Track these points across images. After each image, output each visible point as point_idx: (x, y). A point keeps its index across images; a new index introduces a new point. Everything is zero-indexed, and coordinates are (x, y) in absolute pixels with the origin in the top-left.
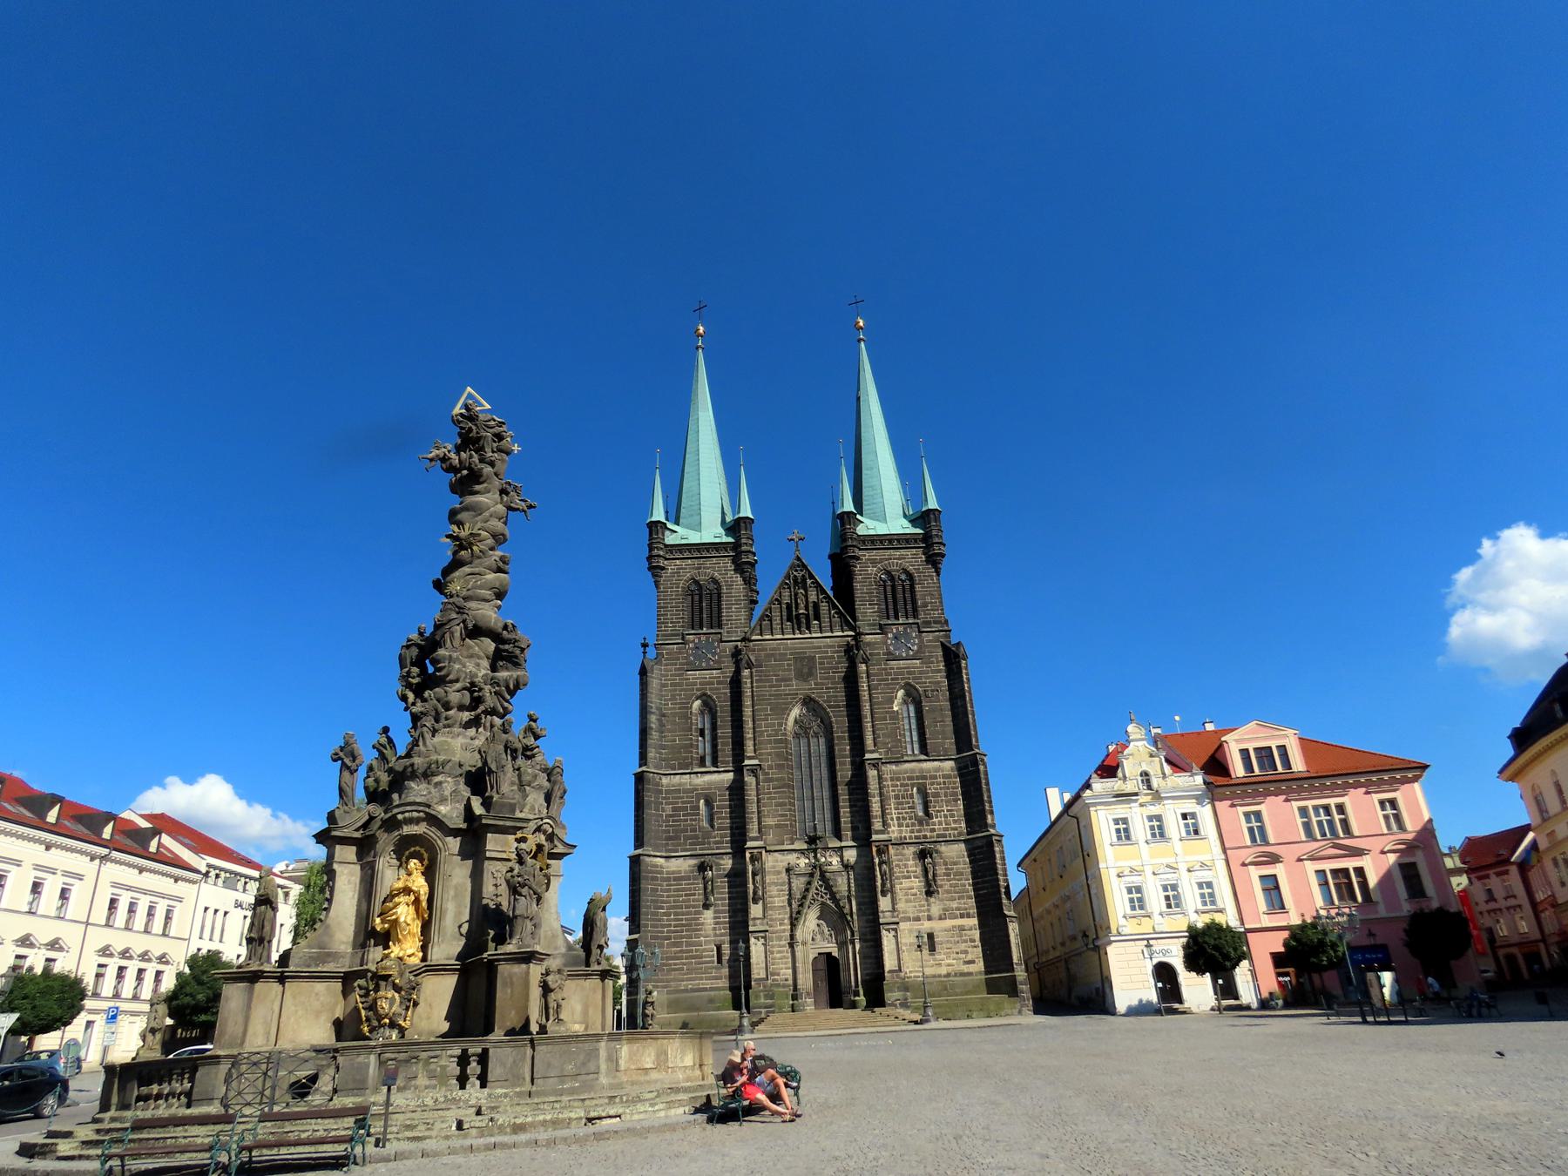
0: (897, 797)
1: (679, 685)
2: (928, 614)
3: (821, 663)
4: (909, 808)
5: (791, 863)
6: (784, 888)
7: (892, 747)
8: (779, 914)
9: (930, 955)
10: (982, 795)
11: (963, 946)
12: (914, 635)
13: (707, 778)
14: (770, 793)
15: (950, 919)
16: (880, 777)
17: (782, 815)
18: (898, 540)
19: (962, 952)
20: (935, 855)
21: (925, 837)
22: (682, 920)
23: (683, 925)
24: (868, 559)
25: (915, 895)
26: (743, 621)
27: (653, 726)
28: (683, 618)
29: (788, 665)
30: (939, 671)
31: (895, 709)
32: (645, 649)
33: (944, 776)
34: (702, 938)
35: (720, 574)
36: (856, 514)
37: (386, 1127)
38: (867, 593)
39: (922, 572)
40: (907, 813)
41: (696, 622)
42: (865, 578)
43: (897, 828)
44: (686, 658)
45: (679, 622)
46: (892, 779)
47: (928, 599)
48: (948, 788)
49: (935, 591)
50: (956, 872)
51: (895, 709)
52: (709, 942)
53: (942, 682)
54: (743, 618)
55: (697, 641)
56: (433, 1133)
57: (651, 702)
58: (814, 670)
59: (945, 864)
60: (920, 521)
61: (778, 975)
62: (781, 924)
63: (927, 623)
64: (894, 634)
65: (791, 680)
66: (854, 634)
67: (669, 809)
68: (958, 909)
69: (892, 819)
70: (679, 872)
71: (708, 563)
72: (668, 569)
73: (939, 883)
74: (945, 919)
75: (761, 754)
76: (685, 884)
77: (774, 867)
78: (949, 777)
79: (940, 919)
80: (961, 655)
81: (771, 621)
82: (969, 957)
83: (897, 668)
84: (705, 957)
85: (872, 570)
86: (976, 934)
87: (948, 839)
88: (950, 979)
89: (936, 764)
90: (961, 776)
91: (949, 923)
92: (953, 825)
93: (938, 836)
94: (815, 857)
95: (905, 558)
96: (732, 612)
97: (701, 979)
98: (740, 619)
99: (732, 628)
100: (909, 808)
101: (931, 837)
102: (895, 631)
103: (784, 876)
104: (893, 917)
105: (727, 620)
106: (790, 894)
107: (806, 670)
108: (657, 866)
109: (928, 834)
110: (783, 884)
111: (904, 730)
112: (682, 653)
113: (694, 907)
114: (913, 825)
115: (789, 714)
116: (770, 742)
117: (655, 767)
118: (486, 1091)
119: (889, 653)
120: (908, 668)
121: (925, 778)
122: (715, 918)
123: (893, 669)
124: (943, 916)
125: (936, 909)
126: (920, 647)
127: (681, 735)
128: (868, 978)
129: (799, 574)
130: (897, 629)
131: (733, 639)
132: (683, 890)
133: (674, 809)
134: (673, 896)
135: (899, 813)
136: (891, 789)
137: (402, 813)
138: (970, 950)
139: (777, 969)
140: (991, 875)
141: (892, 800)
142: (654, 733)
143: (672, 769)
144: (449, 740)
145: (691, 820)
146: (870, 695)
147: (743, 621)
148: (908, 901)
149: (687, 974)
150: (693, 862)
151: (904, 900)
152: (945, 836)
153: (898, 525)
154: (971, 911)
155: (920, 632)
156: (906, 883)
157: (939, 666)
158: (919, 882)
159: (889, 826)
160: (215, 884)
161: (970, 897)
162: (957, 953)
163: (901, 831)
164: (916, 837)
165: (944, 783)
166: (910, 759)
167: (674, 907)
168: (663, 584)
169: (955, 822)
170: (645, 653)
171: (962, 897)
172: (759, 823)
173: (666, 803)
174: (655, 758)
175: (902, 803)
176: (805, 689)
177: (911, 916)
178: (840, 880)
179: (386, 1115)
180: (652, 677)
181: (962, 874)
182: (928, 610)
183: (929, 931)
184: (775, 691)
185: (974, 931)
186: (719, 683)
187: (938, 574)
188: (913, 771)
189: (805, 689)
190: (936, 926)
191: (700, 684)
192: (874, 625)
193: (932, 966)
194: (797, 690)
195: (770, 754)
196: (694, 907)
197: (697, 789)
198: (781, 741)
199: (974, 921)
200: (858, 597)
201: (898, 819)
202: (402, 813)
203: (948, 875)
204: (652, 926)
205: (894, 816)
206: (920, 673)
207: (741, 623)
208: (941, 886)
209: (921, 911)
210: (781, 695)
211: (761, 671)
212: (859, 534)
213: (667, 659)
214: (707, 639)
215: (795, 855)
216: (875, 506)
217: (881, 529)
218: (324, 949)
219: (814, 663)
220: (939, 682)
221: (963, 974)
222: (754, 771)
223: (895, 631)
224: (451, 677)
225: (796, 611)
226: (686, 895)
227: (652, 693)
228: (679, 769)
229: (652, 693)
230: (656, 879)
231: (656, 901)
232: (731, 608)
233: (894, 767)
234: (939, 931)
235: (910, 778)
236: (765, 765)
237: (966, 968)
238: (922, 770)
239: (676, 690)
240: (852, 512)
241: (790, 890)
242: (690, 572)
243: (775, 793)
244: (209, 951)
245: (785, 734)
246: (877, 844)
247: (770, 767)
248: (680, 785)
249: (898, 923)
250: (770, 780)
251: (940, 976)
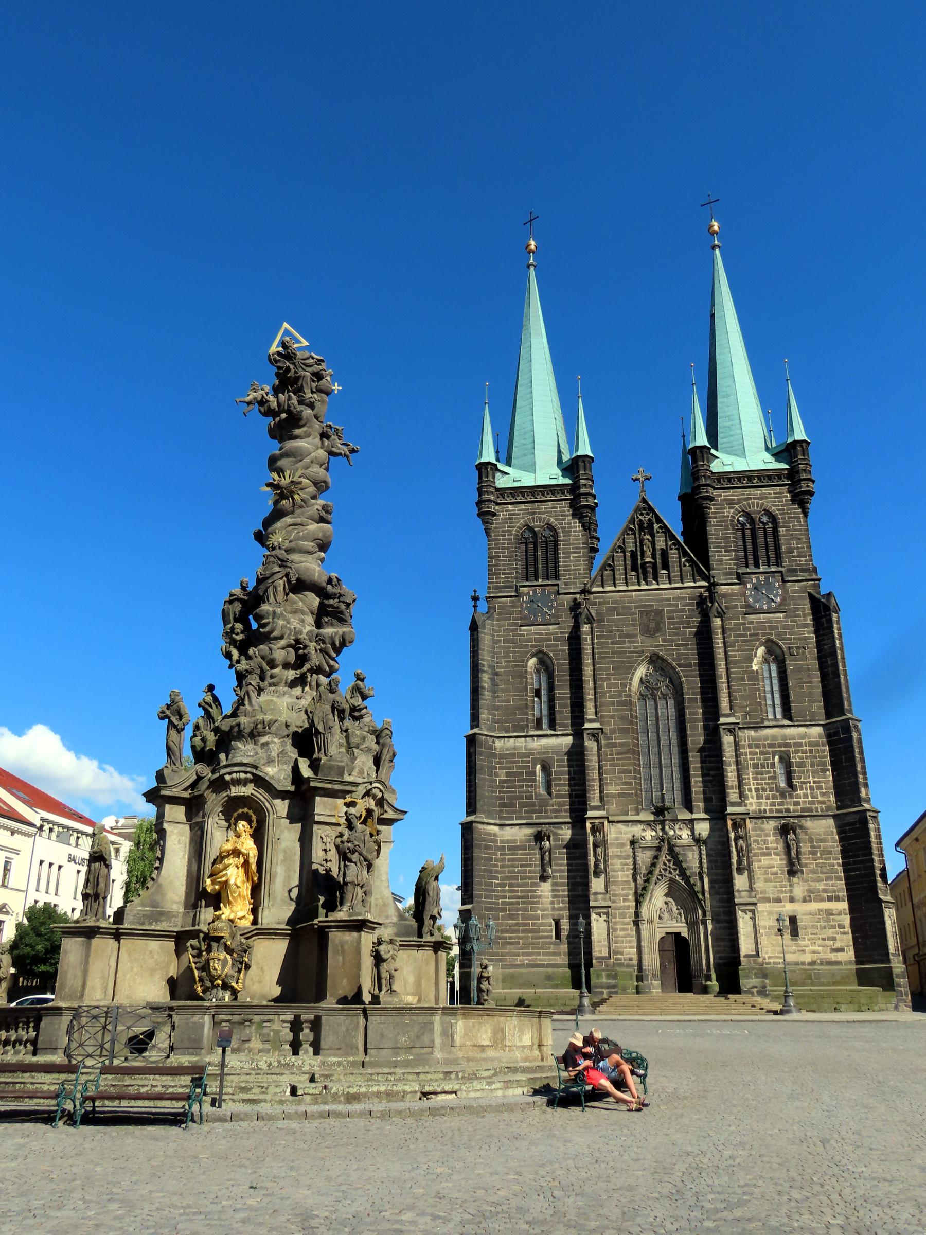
0: (756, 766)
1: (513, 641)
2: (793, 561)
3: (669, 618)
4: (770, 778)
5: (636, 835)
6: (628, 861)
7: (751, 710)
8: (623, 889)
9: (792, 940)
10: (855, 766)
11: (831, 932)
12: (777, 584)
13: (544, 741)
14: (613, 759)
15: (815, 901)
16: (736, 744)
17: (626, 784)
18: (759, 478)
19: (829, 939)
20: (798, 831)
21: (788, 810)
22: (518, 891)
23: (518, 897)
24: (725, 500)
25: (776, 874)
26: (582, 571)
27: (486, 685)
28: (516, 569)
29: (633, 620)
30: (806, 626)
31: (755, 668)
32: (475, 603)
33: (811, 744)
34: (539, 912)
35: (556, 520)
36: (710, 449)
37: (221, 1087)
38: (722, 538)
39: (788, 513)
40: (766, 784)
41: (530, 573)
42: (721, 521)
43: (755, 800)
44: (520, 612)
45: (513, 573)
46: (750, 746)
47: (794, 544)
48: (815, 757)
49: (801, 534)
50: (823, 851)
51: (755, 668)
52: (547, 915)
53: (809, 638)
54: (582, 567)
55: (531, 593)
56: (268, 1097)
57: (483, 660)
58: (662, 625)
59: (811, 840)
60: (785, 454)
61: (622, 953)
62: (624, 900)
63: (793, 571)
64: (753, 584)
65: (635, 636)
66: (706, 584)
67: (503, 775)
68: (825, 891)
69: (750, 790)
70: (515, 841)
71: (543, 507)
72: (499, 515)
73: (803, 861)
75: (602, 717)
76: (521, 854)
77: (617, 839)
78: (816, 744)
79: (804, 901)
80: (832, 607)
81: (613, 570)
82: (838, 945)
83: (757, 623)
84: (544, 932)
85: (728, 512)
86: (846, 920)
87: (814, 813)
88: (815, 967)
89: (802, 730)
90: (830, 743)
91: (814, 906)
92: (820, 799)
93: (803, 810)
94: (663, 829)
95: (766, 498)
96: (570, 561)
97: (539, 954)
98: (580, 570)
99: (570, 579)
100: (770, 778)
101: (794, 811)
102: (754, 581)
103: (628, 848)
104: (750, 897)
105: (564, 570)
106: (635, 869)
107: (653, 625)
108: (490, 834)
109: (792, 808)
110: (627, 857)
111: (765, 692)
112: (516, 607)
113: (530, 878)
114: (774, 797)
115: (633, 674)
116: (613, 704)
117: (488, 730)
118: (319, 1058)
119: (748, 606)
120: (771, 622)
121: (787, 745)
122: (553, 891)
123: (753, 623)
124: (808, 899)
125: (799, 891)
126: (784, 599)
127: (515, 695)
128: (721, 961)
129: (645, 519)
130: (758, 578)
131: (572, 591)
132: (519, 860)
133: (508, 774)
134: (508, 866)
135: (758, 784)
136: (749, 757)
137: (230, 774)
138: (838, 936)
139: (621, 947)
140: (864, 855)
141: (751, 770)
142: (486, 693)
143: (507, 731)
144: (274, 699)
145: (527, 786)
146: (726, 652)
147: (582, 571)
148: (767, 880)
149: (522, 949)
150: (530, 831)
151: (762, 879)
152: (810, 810)
153: (761, 460)
154: (841, 894)
155: (784, 581)
156: (765, 861)
157: (805, 620)
158: (781, 860)
159: (747, 798)
160: (49, 838)
161: (839, 879)
162: (824, 939)
163: (760, 804)
164: (778, 811)
165: (811, 751)
166: (771, 724)
167: (509, 878)
168: (494, 532)
169: (823, 794)
170: (475, 607)
171: (827, 879)
172: (601, 792)
173: (500, 768)
174: (488, 720)
175: (762, 773)
176: (652, 646)
177: (771, 896)
178: (690, 855)
179: (222, 1075)
180: (484, 633)
181: (830, 853)
182: (793, 556)
183: (791, 914)
184: (618, 648)
185: (843, 917)
186: (556, 639)
187: (806, 514)
188: (774, 737)
189: (652, 646)
190: (798, 908)
191: (536, 640)
192: (731, 574)
193: (795, 953)
194: (643, 647)
195: (613, 717)
196: (530, 878)
197: (533, 754)
198: (624, 703)
199: (844, 905)
200: (711, 543)
201: (757, 790)
202: (230, 774)
203: (814, 853)
204: (487, 897)
205: (753, 787)
206: (784, 627)
207: (579, 574)
208: (806, 865)
209: (782, 892)
210: (625, 652)
211: (603, 627)
212: (714, 470)
213: (500, 613)
214: (543, 592)
215: (640, 827)
216: (731, 439)
217: (739, 465)
218: (158, 907)
219: (662, 617)
220: (805, 639)
221: (830, 963)
222: (595, 735)
223: (754, 581)
224: (275, 634)
225: (642, 559)
226: (522, 866)
227: (484, 650)
228: (513, 732)
229: (484, 650)
230: (490, 847)
231: (490, 871)
232: (569, 557)
233: (752, 733)
234: (803, 915)
235: (770, 746)
236: (607, 729)
237: (833, 957)
238: (785, 737)
239: (509, 647)
240: (705, 447)
241: (635, 864)
242: (523, 518)
243: (618, 759)
244: (45, 903)
245: (630, 696)
246: (733, 817)
247: (613, 731)
248: (515, 748)
249: (756, 904)
250: (614, 745)
251: (803, 963)
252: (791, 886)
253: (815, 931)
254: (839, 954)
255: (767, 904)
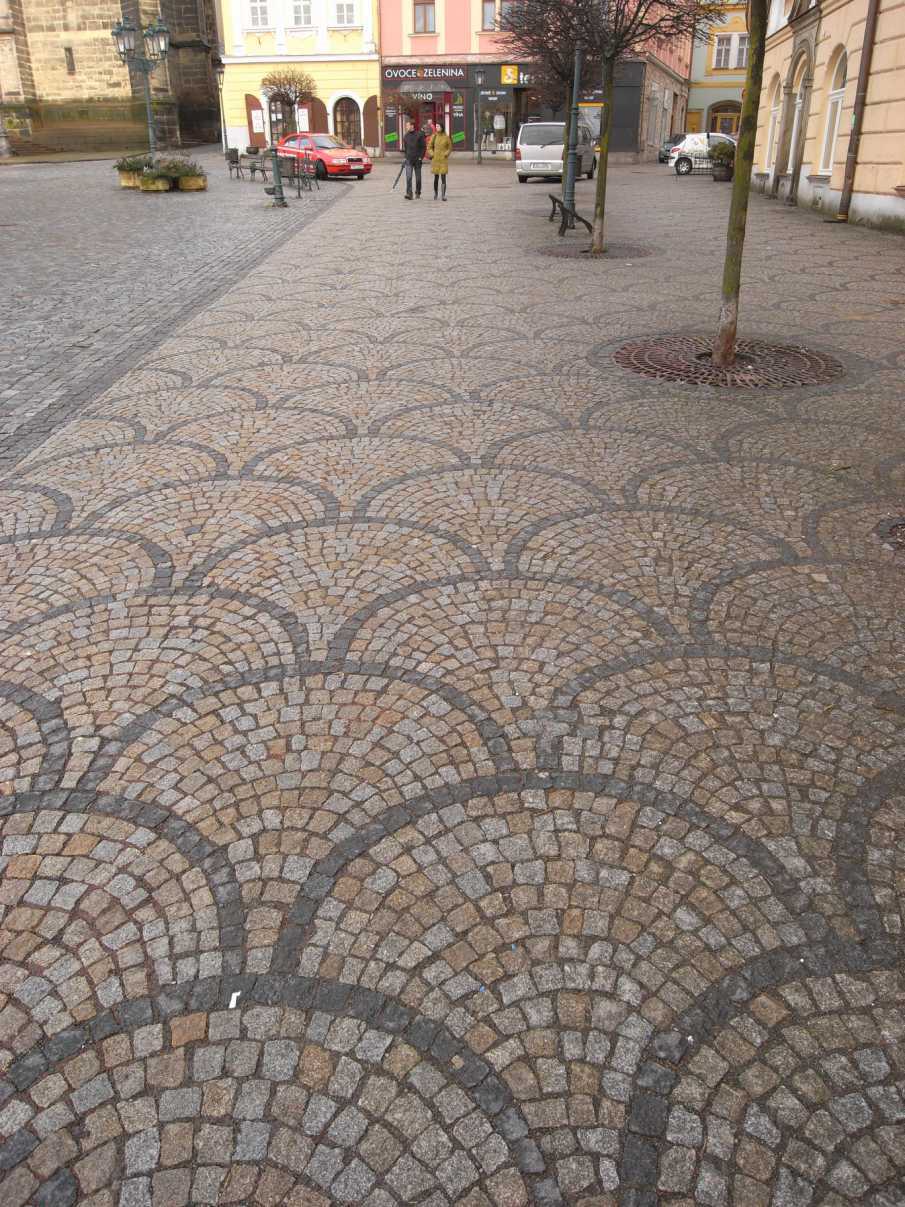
68: (100, 17)
74: (85, 29)
79: (79, 29)
82: (115, 79)
91: (89, 35)
138: (115, 70)
162: (100, 73)
177: (44, 24)
183: (67, 45)
190: (75, 38)
209: (55, 18)
234: (79, 45)
252: (65, 11)
253: (91, 64)
254: (116, 89)
255: (41, 33)
